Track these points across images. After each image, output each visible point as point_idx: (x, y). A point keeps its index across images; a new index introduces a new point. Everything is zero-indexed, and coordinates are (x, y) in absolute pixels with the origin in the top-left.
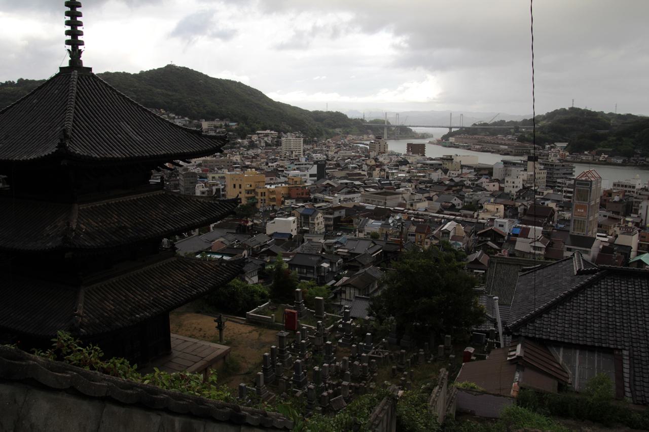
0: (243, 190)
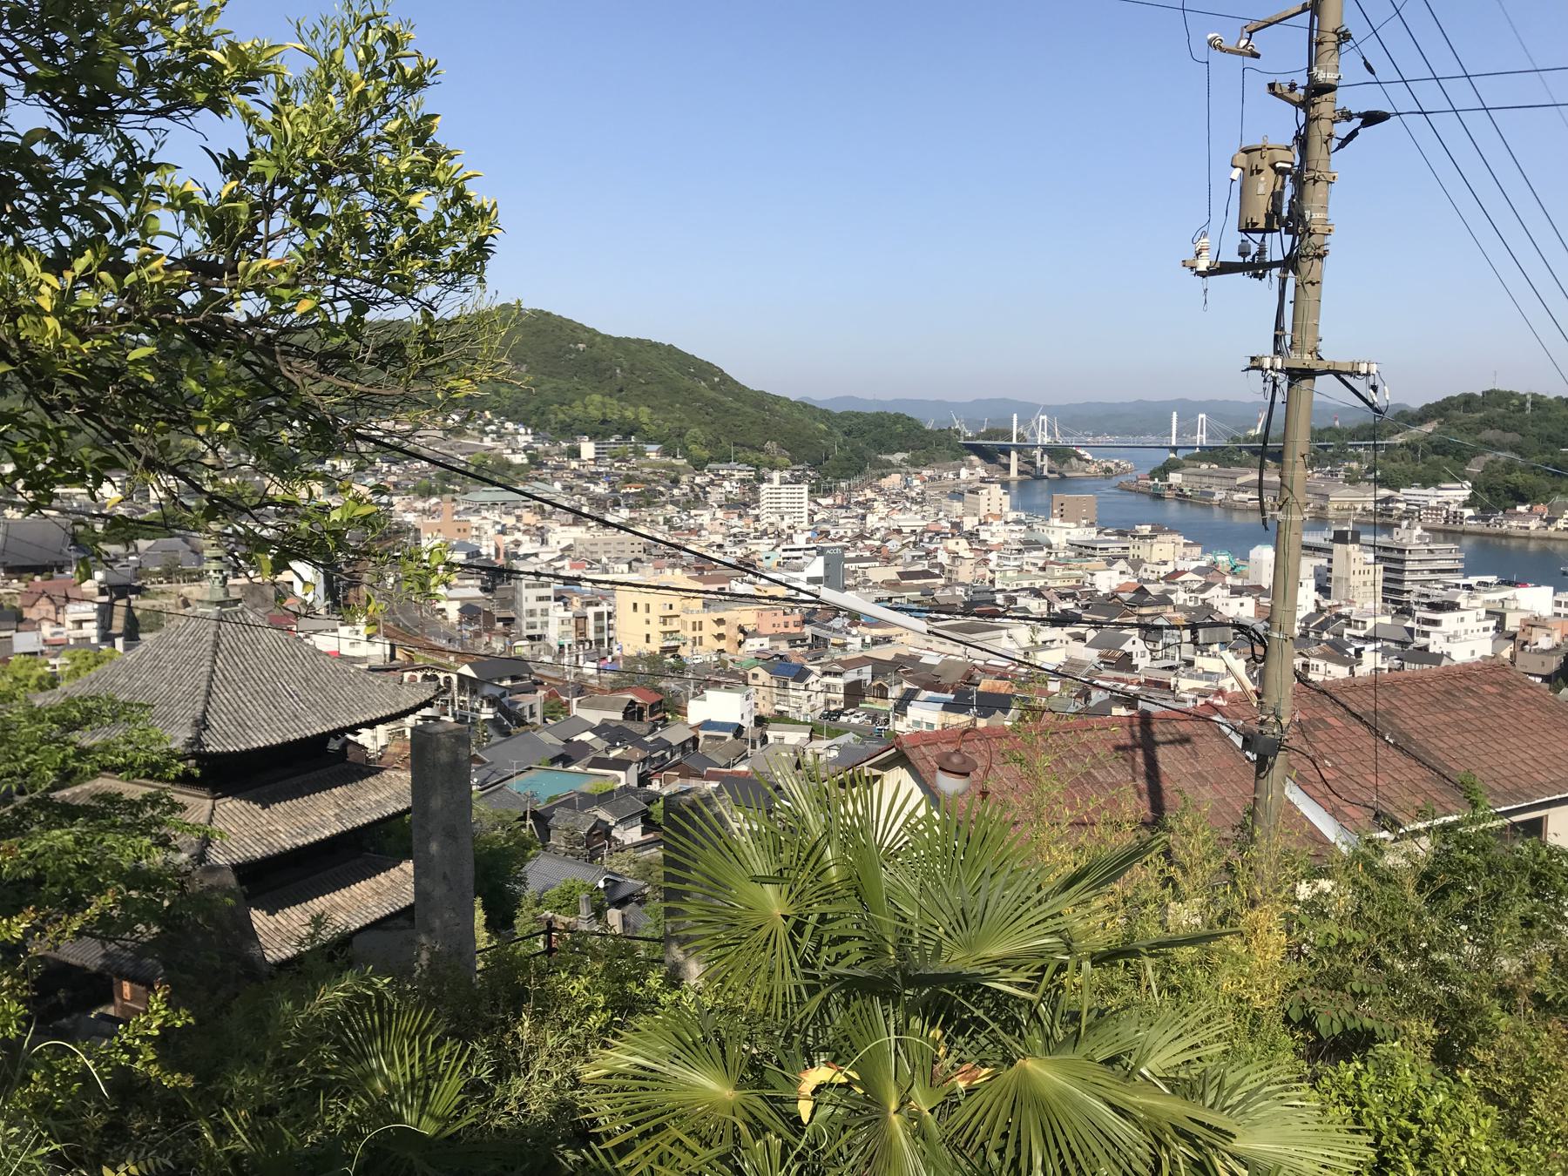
0: (654, 616)
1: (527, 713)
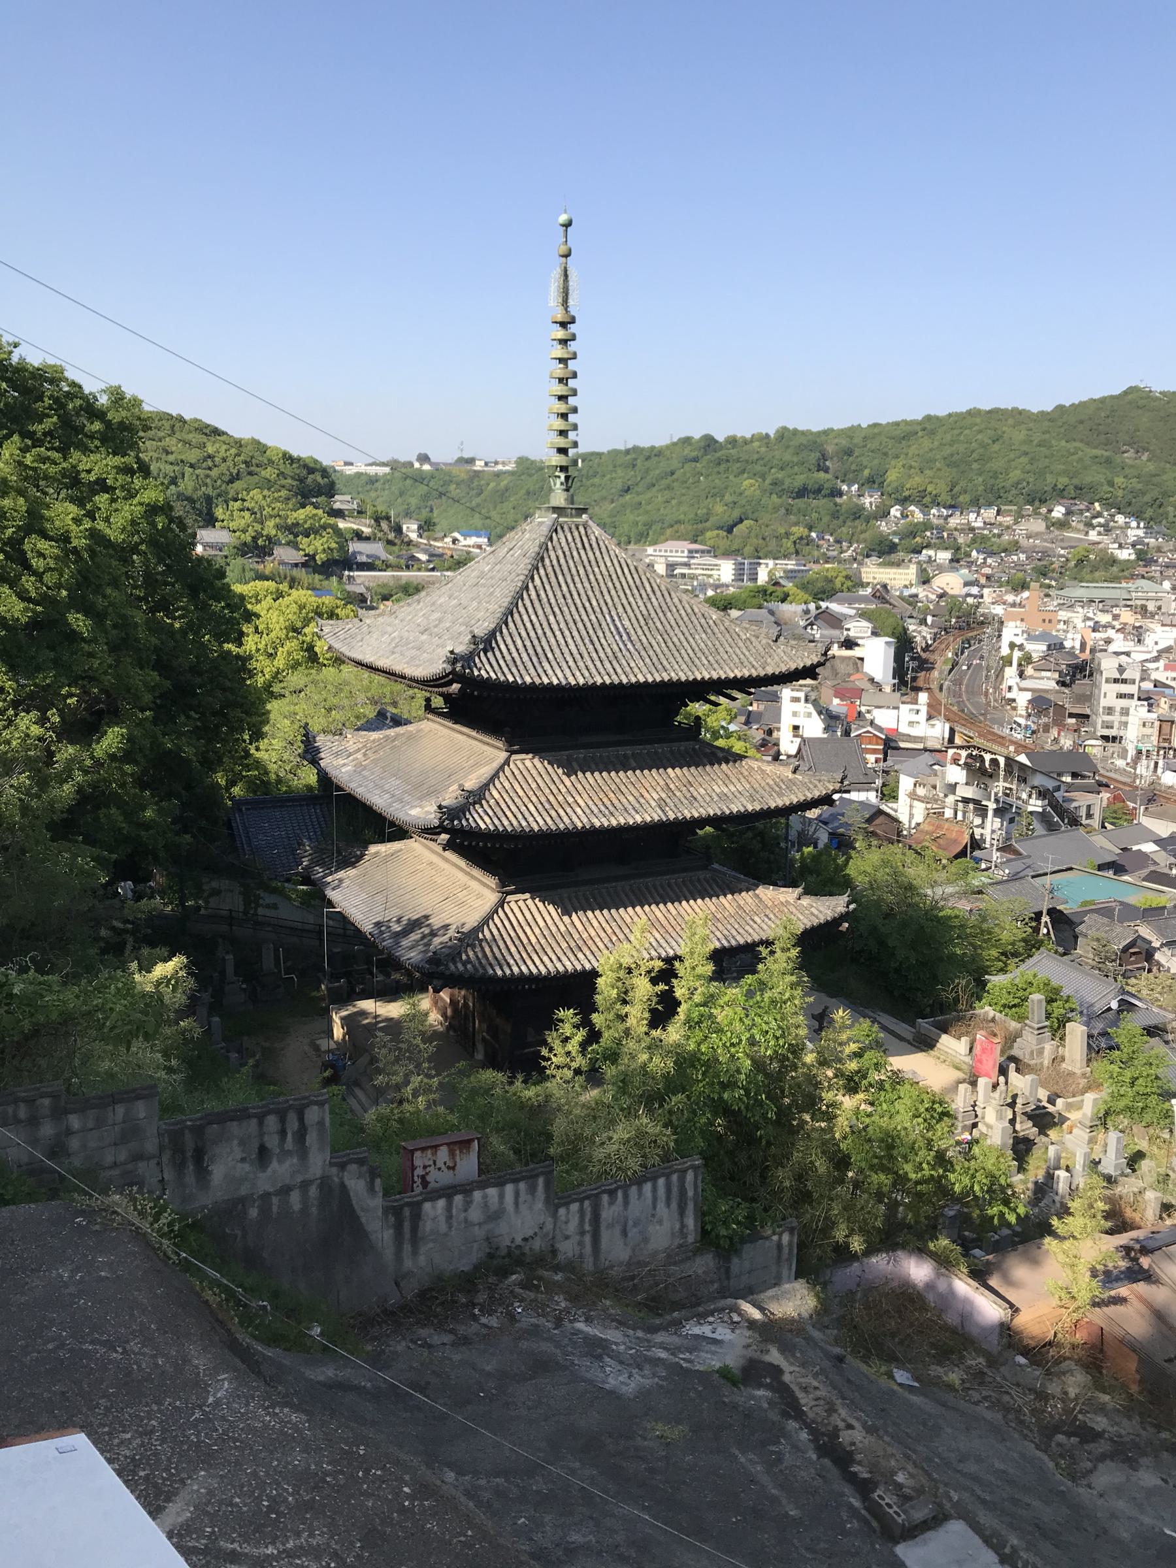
1: (1083, 812)
